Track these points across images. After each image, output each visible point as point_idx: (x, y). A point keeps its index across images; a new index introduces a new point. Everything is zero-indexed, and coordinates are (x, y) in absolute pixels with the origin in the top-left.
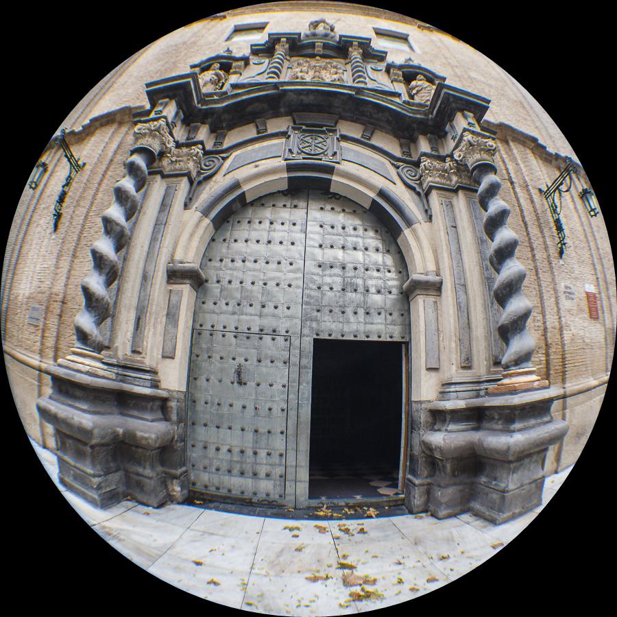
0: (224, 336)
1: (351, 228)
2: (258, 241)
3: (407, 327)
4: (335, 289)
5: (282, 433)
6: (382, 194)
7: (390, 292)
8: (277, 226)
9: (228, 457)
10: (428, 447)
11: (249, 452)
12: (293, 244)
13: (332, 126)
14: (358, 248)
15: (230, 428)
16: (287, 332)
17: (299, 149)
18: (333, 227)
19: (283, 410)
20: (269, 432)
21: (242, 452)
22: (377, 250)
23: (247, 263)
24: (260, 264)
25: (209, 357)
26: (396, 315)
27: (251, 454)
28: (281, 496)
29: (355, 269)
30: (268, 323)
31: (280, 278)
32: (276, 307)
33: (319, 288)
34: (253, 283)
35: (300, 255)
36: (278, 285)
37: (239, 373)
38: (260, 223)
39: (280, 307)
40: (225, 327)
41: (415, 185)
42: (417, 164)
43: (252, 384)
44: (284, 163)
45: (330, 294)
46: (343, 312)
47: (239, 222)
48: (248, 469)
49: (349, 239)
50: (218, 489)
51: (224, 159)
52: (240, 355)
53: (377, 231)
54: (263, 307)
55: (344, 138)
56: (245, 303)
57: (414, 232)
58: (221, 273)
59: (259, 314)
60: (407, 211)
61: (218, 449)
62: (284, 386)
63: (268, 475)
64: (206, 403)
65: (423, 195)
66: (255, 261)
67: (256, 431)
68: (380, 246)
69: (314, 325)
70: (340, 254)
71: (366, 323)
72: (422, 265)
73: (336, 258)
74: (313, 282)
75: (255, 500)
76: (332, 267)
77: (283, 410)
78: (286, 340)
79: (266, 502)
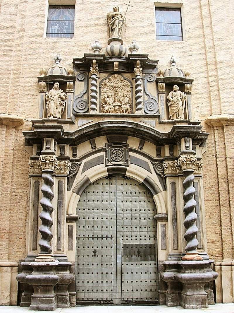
0: (88, 239)
1: (134, 193)
2: (98, 201)
3: (156, 232)
4: (128, 219)
5: (111, 273)
6: (146, 180)
7: (149, 219)
8: (105, 194)
9: (92, 284)
10: (162, 277)
11: (100, 282)
12: (111, 201)
13: (126, 143)
14: (137, 201)
15: (93, 273)
16: (111, 236)
17: (112, 159)
18: (127, 193)
19: (111, 265)
20: (107, 273)
21: (97, 282)
22: (144, 202)
23: (94, 210)
24: (100, 211)
25: (84, 247)
26: (152, 227)
27: (101, 282)
28: (111, 299)
29: (136, 210)
30: (105, 233)
31: (107, 216)
32: (107, 227)
33: (122, 219)
34: (98, 218)
35: (115, 206)
36: (107, 218)
37: (95, 252)
38: (98, 192)
39: (108, 227)
40: (88, 236)
41: (161, 174)
42: (162, 161)
43: (100, 256)
44: (106, 168)
45: (126, 221)
46: (131, 228)
47: (89, 192)
48: (99, 289)
49: (133, 197)
50: (88, 299)
51: (80, 165)
52: (95, 246)
53: (144, 193)
54: (102, 227)
55: (131, 150)
56: (95, 226)
57: (158, 196)
58: (85, 215)
59: (101, 230)
60: (156, 187)
61: (88, 282)
62: (111, 256)
63: (107, 290)
64: (83, 265)
65: (163, 179)
66: (98, 210)
67: (102, 273)
68: (146, 200)
69: (121, 233)
70: (129, 204)
71: (140, 232)
72: (161, 210)
73: (128, 206)
74: (120, 217)
75: (102, 302)
76: (127, 210)
77: (111, 265)
78: (111, 239)
79: (106, 302)
